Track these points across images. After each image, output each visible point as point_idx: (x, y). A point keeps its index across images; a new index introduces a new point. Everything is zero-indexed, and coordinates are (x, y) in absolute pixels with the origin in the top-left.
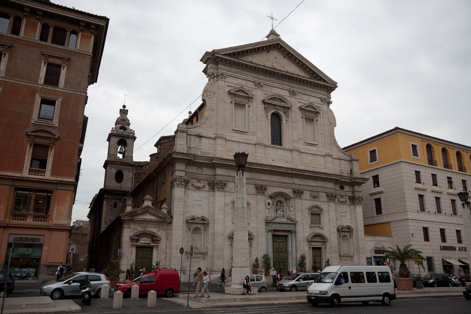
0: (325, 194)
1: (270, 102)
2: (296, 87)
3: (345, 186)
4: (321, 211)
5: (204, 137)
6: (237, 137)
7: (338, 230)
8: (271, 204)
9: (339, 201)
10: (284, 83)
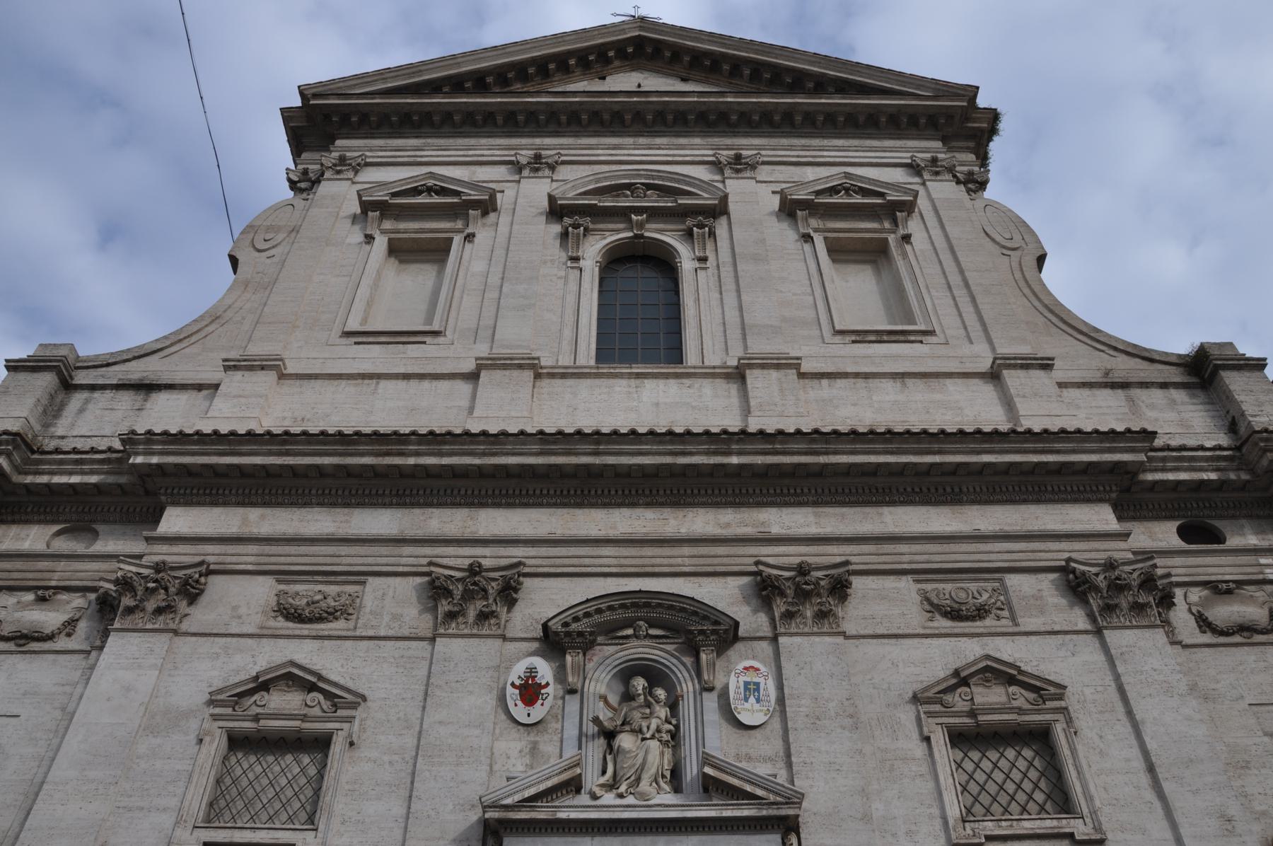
4: (1050, 704)
5: (170, 387)
8: (550, 690)
9: (1204, 623)
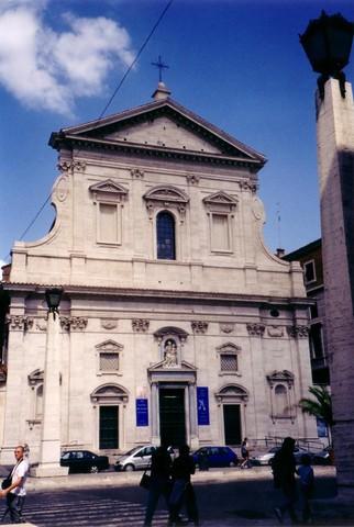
0: (245, 326)
1: (152, 197)
2: (197, 171)
3: (280, 312)
6: (105, 253)
7: (268, 378)
9: (269, 334)
10: (178, 165)
